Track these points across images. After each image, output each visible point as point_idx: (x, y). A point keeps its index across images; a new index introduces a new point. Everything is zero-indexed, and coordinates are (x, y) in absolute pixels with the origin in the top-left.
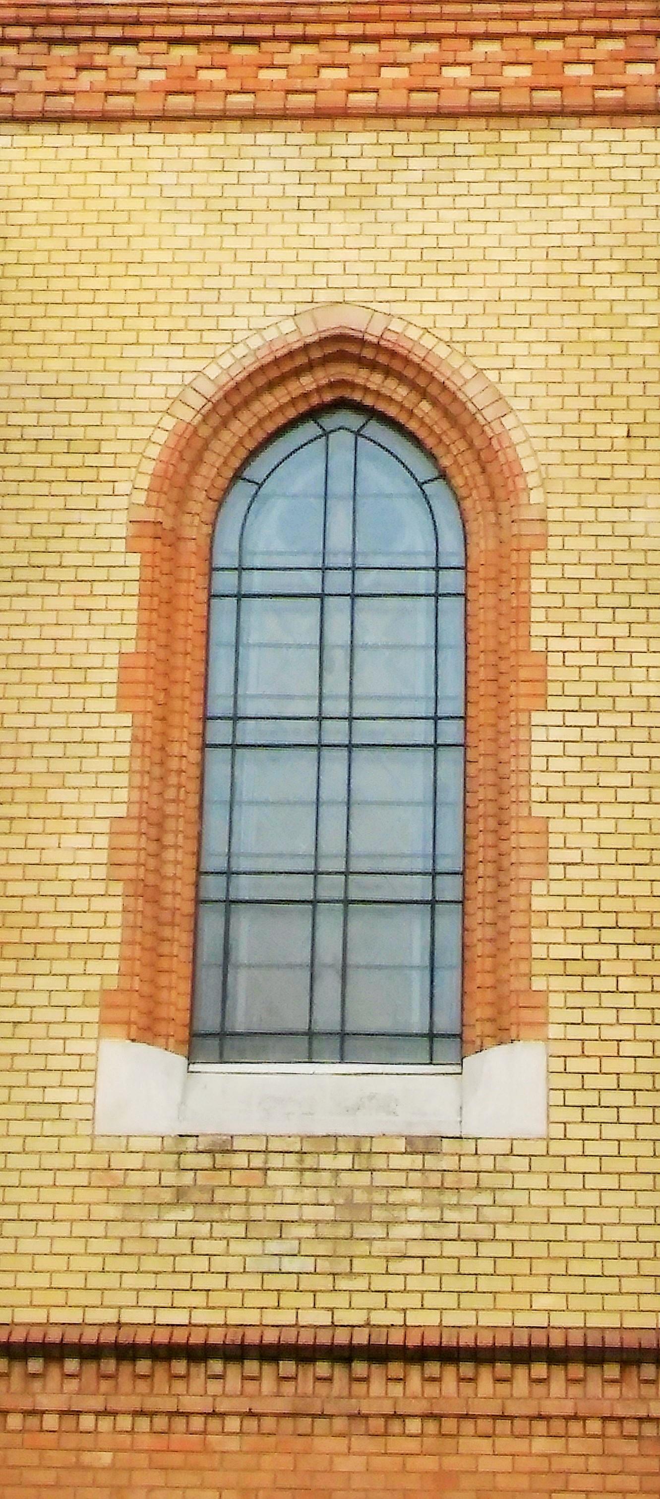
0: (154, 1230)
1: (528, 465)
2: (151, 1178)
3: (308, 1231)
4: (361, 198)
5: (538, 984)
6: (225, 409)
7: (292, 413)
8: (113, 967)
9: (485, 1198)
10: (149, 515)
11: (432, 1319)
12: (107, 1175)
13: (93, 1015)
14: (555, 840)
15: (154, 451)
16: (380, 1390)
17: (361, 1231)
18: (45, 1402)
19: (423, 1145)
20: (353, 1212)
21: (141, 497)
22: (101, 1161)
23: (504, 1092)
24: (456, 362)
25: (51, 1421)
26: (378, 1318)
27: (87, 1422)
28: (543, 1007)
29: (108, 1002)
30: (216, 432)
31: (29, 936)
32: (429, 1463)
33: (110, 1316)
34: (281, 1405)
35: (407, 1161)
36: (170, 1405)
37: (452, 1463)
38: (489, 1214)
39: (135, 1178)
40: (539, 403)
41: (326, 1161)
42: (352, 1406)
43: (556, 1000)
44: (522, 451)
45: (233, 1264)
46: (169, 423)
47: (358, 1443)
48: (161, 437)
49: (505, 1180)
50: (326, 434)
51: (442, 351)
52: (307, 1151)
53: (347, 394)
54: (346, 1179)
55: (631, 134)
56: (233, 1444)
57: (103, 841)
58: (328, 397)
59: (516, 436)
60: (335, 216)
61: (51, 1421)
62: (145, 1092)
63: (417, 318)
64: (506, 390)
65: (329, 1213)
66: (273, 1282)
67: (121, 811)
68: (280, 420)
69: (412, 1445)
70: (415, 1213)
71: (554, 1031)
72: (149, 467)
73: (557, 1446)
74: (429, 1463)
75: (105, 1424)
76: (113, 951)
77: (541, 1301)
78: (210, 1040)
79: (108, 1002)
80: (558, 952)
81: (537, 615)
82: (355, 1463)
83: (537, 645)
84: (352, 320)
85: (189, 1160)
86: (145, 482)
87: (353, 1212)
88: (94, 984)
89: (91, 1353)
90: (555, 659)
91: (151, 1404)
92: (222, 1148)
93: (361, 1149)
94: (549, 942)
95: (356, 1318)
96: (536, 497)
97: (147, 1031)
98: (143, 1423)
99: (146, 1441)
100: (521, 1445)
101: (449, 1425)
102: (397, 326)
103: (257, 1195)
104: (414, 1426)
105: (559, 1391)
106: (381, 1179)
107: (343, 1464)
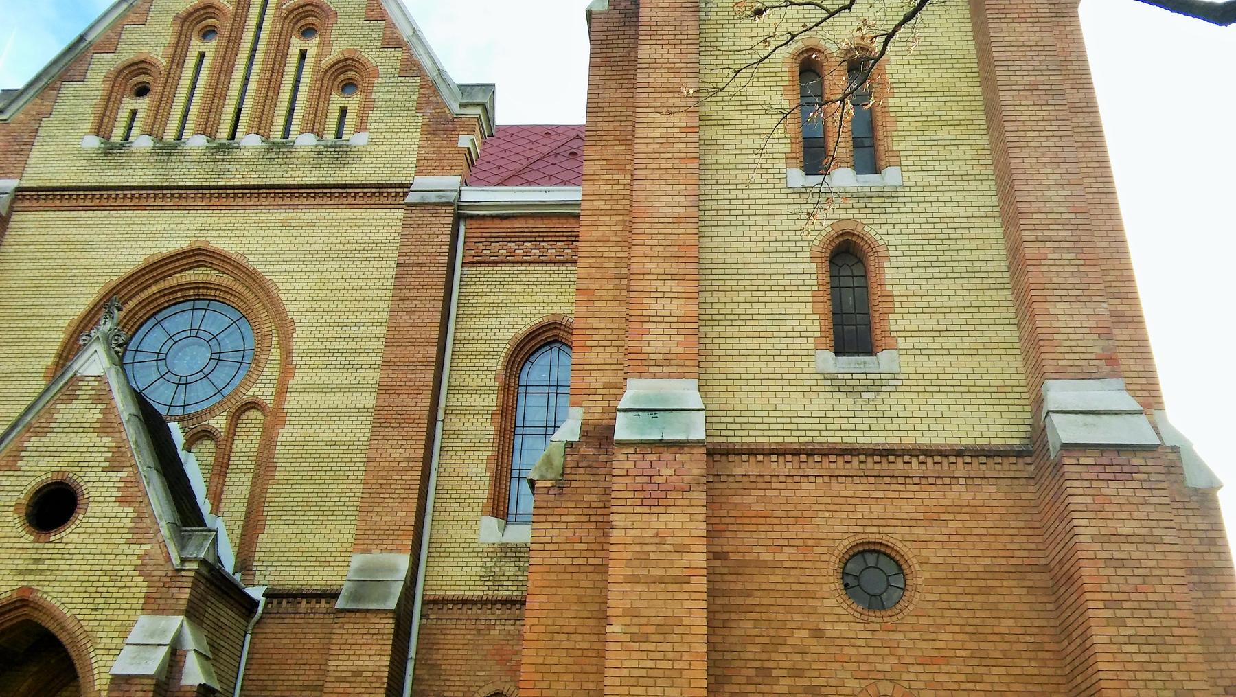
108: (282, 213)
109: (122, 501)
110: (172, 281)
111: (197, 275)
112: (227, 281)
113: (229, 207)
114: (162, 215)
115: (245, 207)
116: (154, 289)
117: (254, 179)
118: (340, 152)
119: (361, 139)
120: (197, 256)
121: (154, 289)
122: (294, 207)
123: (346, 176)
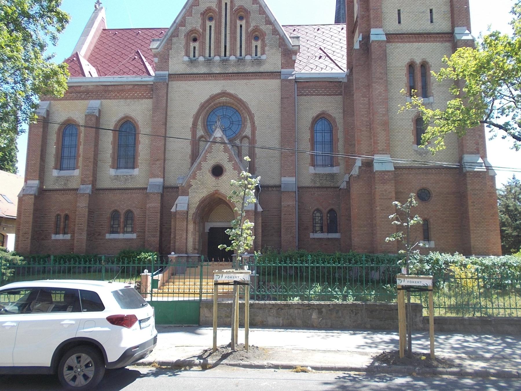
4: (129, 105)
16: (127, 191)
20: (126, 180)
23: (136, 172)
52: (123, 176)
62: (112, 172)
63: (133, 115)
78: (118, 168)
87: (126, 180)
92: (118, 176)
93: (127, 176)
94: (139, 161)
108: (245, 81)
109: (234, 169)
110: (217, 101)
111: (223, 99)
112: (232, 101)
113: (230, 79)
114: (210, 82)
115: (234, 79)
116: (212, 104)
117: (235, 70)
118: (258, 62)
119: (264, 57)
120: (224, 94)
121: (212, 104)
122: (248, 79)
123: (262, 69)
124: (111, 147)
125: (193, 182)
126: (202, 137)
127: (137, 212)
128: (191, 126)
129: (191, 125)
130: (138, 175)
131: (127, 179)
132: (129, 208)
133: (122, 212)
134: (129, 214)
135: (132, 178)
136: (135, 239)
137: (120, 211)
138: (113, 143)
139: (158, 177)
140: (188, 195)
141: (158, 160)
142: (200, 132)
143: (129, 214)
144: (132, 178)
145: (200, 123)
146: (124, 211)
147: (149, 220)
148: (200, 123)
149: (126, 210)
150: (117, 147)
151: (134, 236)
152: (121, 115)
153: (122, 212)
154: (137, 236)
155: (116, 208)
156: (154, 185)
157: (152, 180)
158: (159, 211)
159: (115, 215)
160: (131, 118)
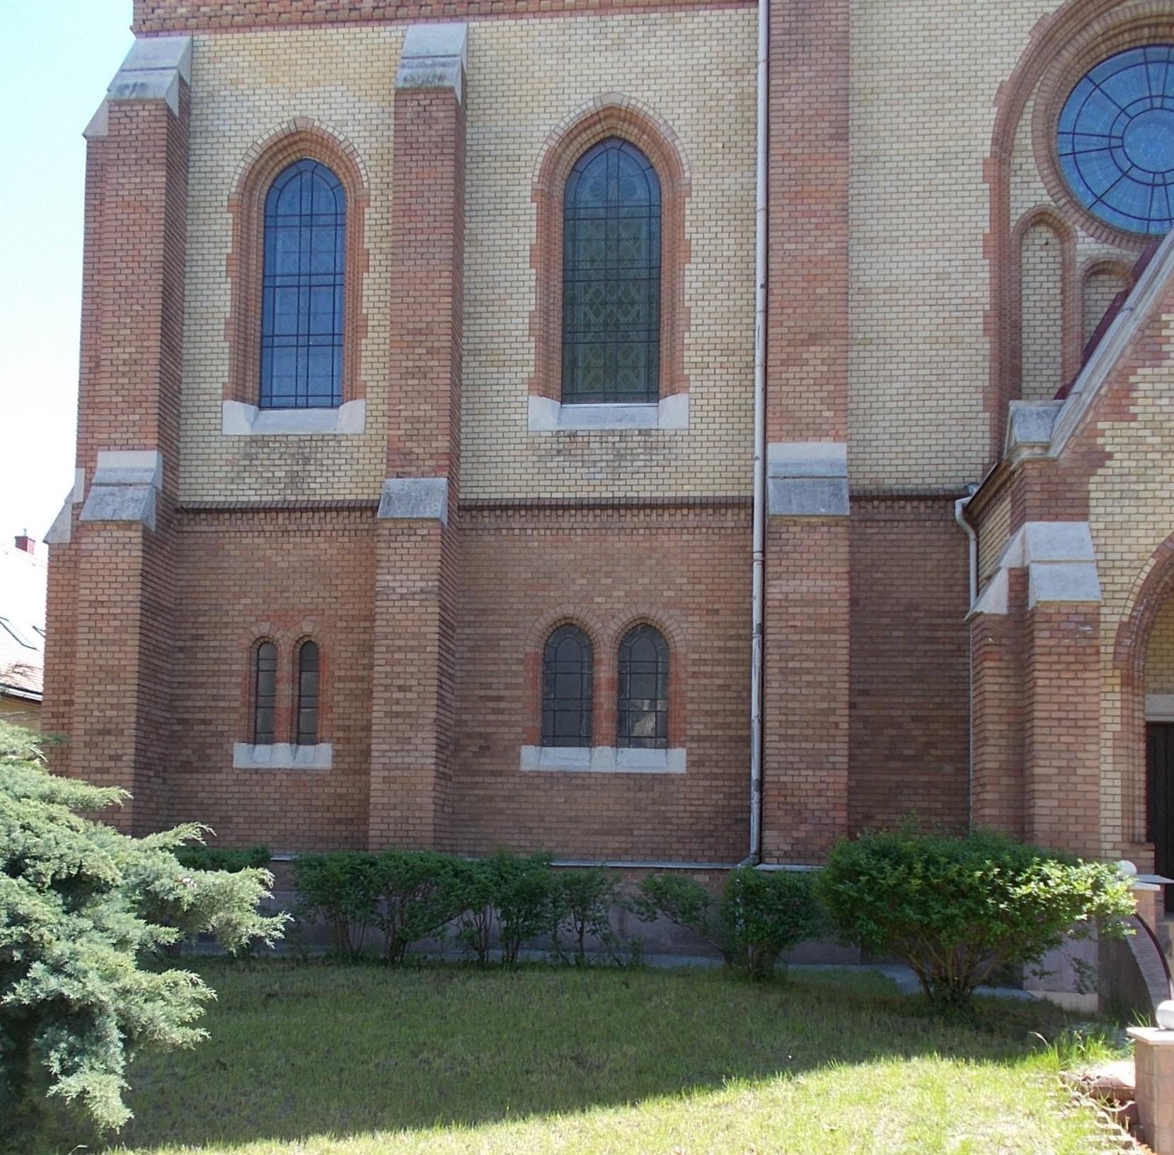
0: (549, 465)
1: (684, 161)
2: (549, 446)
3: (604, 464)
4: (619, 45)
5: (686, 372)
6: (567, 140)
7: (593, 142)
8: (533, 369)
9: (667, 451)
10: (540, 187)
11: (648, 495)
12: (533, 446)
13: (526, 387)
14: (693, 316)
15: (540, 159)
16: (630, 519)
17: (623, 464)
18: (514, 525)
19: (644, 433)
20: (620, 457)
21: (536, 179)
22: (530, 440)
23: (673, 412)
24: (656, 117)
25: (517, 532)
26: (629, 494)
27: (529, 532)
28: (688, 380)
29: (530, 382)
30: (564, 151)
31: (501, 358)
32: (647, 544)
33: (536, 495)
34: (595, 525)
35: (639, 438)
36: (557, 526)
37: (654, 544)
38: (668, 457)
39: (543, 446)
40: (689, 134)
41: (610, 439)
42: (620, 525)
43: (692, 378)
44: (682, 155)
45: (578, 476)
46: (546, 147)
47: (622, 538)
48: (543, 153)
49: (674, 445)
50: (606, 150)
51: (651, 112)
52: (603, 435)
53: (614, 132)
54: (617, 445)
55: (727, 12)
56: (579, 539)
57: (527, 320)
58: (607, 134)
59: (680, 148)
60: (609, 54)
61: (517, 532)
62: (544, 414)
63: (642, 97)
64: (676, 129)
65: (611, 457)
66: (592, 482)
67: (533, 308)
68: (589, 145)
69: (641, 538)
70: (642, 457)
71: (692, 390)
72: (538, 166)
73: (691, 537)
74: (647, 544)
75: (535, 532)
76: (532, 363)
77: (686, 487)
78: (568, 396)
79: (530, 382)
80: (693, 360)
81: (687, 224)
82: (622, 544)
83: (687, 236)
84: (616, 100)
85: (561, 440)
86: (537, 173)
87: (620, 457)
88: (526, 375)
89: (528, 508)
90: (694, 242)
91: (550, 525)
92: (573, 435)
93: (623, 435)
94: (690, 357)
95: (622, 495)
96: (687, 174)
97: (545, 394)
98: (548, 532)
99: (550, 538)
100: (678, 538)
101: (654, 531)
102: (633, 102)
103: (586, 452)
104: (642, 532)
105: (692, 518)
106: (630, 445)
107: (617, 545)
124: (529, 276)
125: (1111, 435)
126: (1040, 218)
127: (685, 633)
128: (986, 149)
129: (985, 148)
130: (687, 432)
131: (620, 450)
132: (643, 610)
133: (606, 634)
134: (643, 636)
135: (650, 448)
136: (682, 777)
137: (594, 624)
138: (541, 256)
139: (819, 434)
140: (1084, 517)
141: (813, 338)
142: (1032, 192)
143: (643, 636)
144: (650, 448)
145: (1025, 137)
146: (614, 627)
147: (785, 672)
148: (1025, 137)
149: (625, 618)
150: (557, 285)
151: (675, 761)
152: (577, 102)
153: (606, 634)
154: (691, 764)
155: (569, 610)
156: (801, 479)
157: (784, 452)
158: (842, 622)
159: (567, 642)
160: (629, 116)
